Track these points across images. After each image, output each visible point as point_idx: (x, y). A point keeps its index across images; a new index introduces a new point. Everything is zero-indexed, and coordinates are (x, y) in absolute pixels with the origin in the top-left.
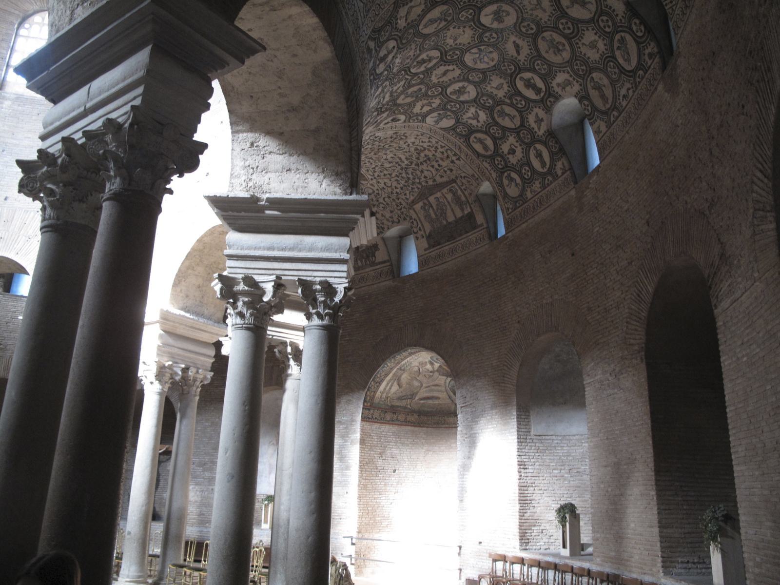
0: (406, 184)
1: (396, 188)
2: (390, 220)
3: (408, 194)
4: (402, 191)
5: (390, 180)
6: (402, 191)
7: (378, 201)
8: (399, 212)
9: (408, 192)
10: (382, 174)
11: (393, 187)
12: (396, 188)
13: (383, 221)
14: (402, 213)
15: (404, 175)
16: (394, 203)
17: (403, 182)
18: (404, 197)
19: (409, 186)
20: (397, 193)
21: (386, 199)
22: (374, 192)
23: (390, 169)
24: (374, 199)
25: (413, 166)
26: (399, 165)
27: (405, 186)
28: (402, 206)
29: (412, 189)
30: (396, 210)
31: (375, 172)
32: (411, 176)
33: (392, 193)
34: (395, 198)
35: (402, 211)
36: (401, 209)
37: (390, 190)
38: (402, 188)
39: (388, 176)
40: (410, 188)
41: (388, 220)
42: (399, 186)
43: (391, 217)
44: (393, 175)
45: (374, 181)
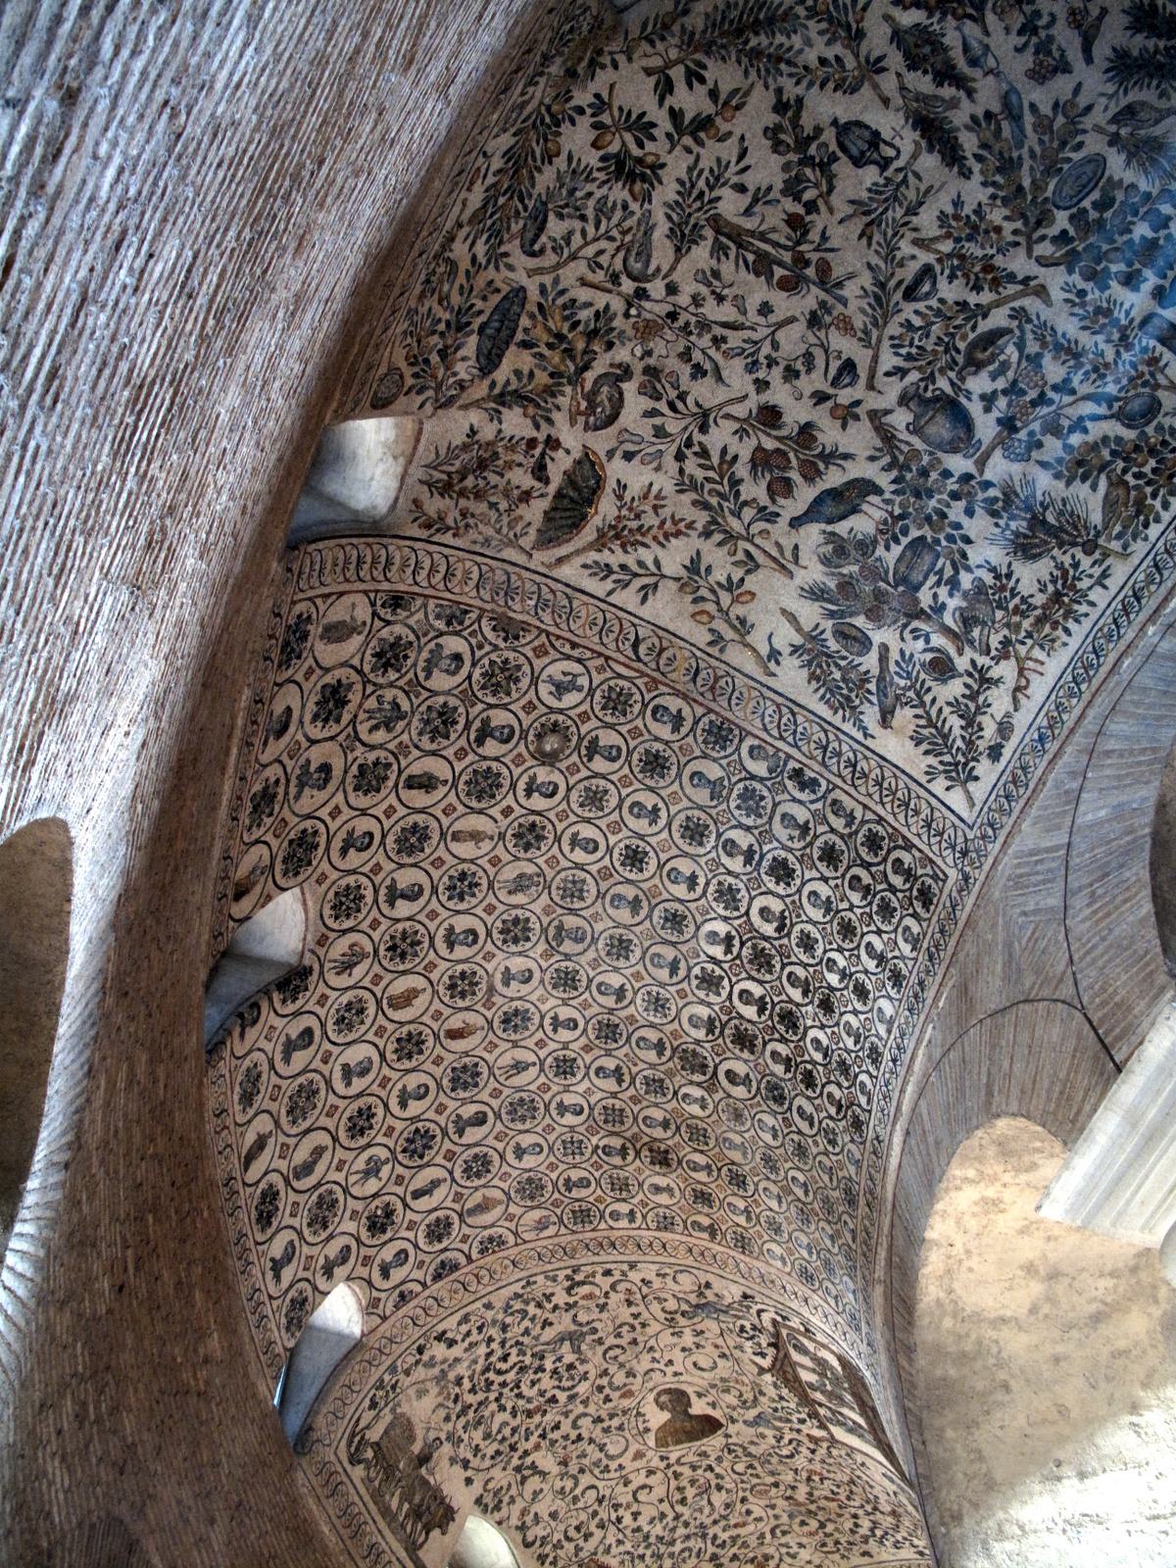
0: (652, 1540)
1: (636, 1515)
2: (529, 1519)
3: (622, 1549)
4: (628, 1532)
5: (661, 1501)
6: (628, 1532)
7: (582, 1471)
8: (558, 1536)
9: (628, 1546)
10: (685, 1483)
11: (634, 1508)
12: (636, 1515)
13: (518, 1499)
14: (558, 1546)
15: (681, 1531)
16: (583, 1517)
17: (658, 1530)
18: (611, 1540)
19: (647, 1547)
20: (619, 1520)
21: (592, 1495)
22: (611, 1458)
23: (704, 1502)
24: (586, 1461)
25: (711, 1549)
26: (715, 1522)
27: (647, 1537)
28: (581, 1542)
29: (642, 1557)
30: (562, 1527)
31: (694, 1468)
32: (678, 1547)
33: (616, 1507)
34: (603, 1515)
35: (565, 1544)
36: (569, 1539)
37: (625, 1498)
38: (638, 1529)
39: (678, 1496)
40: (641, 1551)
41: (524, 1512)
42: (642, 1521)
43: (537, 1518)
44: (679, 1508)
45: (656, 1462)
